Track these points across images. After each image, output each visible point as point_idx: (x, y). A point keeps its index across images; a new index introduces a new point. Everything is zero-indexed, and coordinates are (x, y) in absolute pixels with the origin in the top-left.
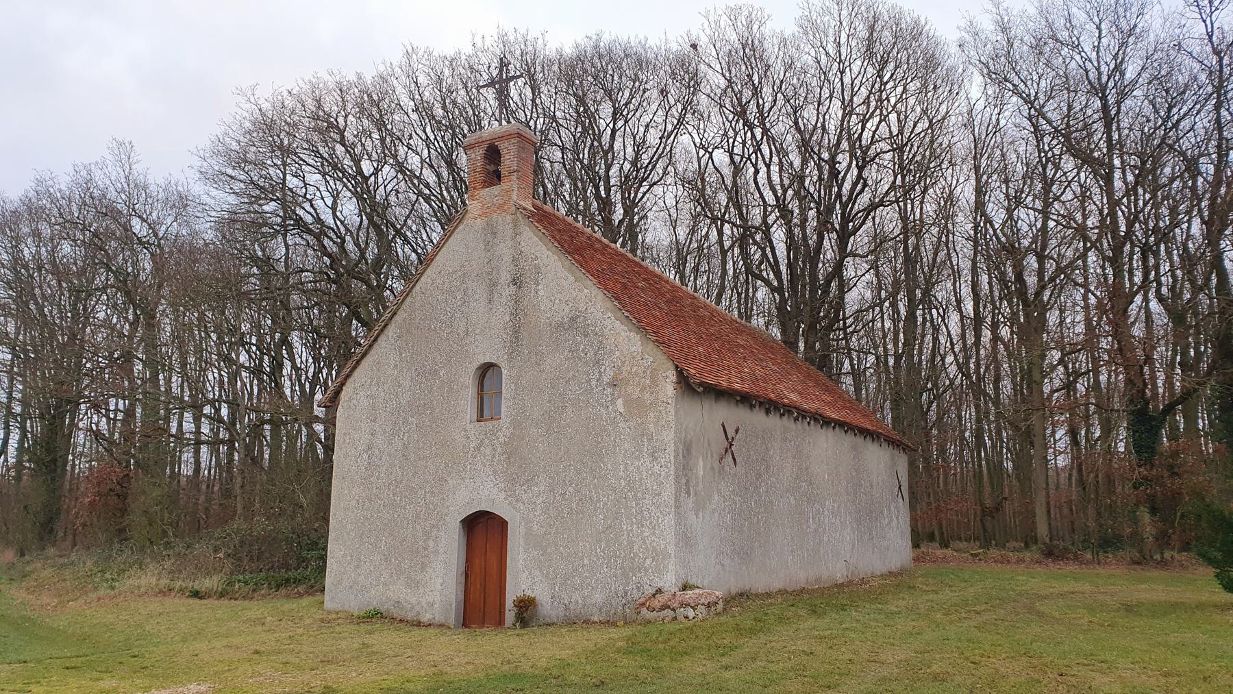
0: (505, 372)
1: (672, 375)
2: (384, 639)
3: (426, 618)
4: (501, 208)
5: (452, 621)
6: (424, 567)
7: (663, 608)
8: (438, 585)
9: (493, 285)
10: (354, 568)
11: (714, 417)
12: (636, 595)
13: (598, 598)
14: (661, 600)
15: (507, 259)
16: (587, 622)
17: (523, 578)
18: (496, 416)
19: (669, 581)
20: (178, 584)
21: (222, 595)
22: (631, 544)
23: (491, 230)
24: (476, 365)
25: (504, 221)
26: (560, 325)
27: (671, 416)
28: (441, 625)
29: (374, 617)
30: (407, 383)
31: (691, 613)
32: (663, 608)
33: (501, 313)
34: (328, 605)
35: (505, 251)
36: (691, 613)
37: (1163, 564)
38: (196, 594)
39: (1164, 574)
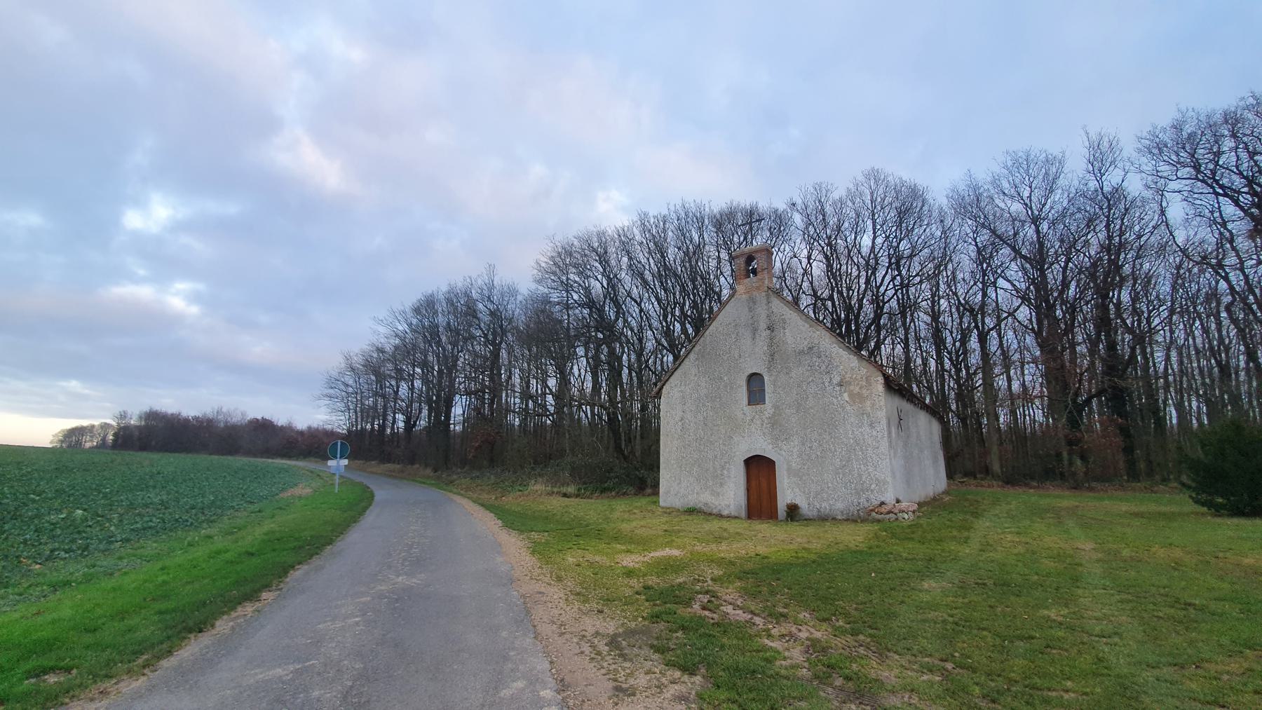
0: (766, 378)
1: (881, 379)
2: (694, 525)
3: (725, 513)
4: (758, 288)
5: (743, 514)
6: (721, 485)
7: (889, 513)
8: (732, 494)
9: (755, 331)
10: (675, 485)
11: (897, 402)
12: (866, 505)
13: (840, 506)
14: (884, 509)
15: (763, 316)
16: (834, 519)
17: (787, 492)
18: (763, 401)
19: (889, 497)
20: (555, 490)
21: (577, 496)
22: (860, 476)
23: (752, 301)
24: (747, 374)
25: (760, 296)
26: (802, 352)
27: (882, 403)
28: (736, 517)
29: (691, 511)
30: (703, 384)
31: (906, 516)
32: (889, 513)
33: (762, 345)
34: (662, 504)
35: (761, 311)
36: (906, 516)
37: (1091, 489)
38: (565, 495)
39: (1091, 494)
